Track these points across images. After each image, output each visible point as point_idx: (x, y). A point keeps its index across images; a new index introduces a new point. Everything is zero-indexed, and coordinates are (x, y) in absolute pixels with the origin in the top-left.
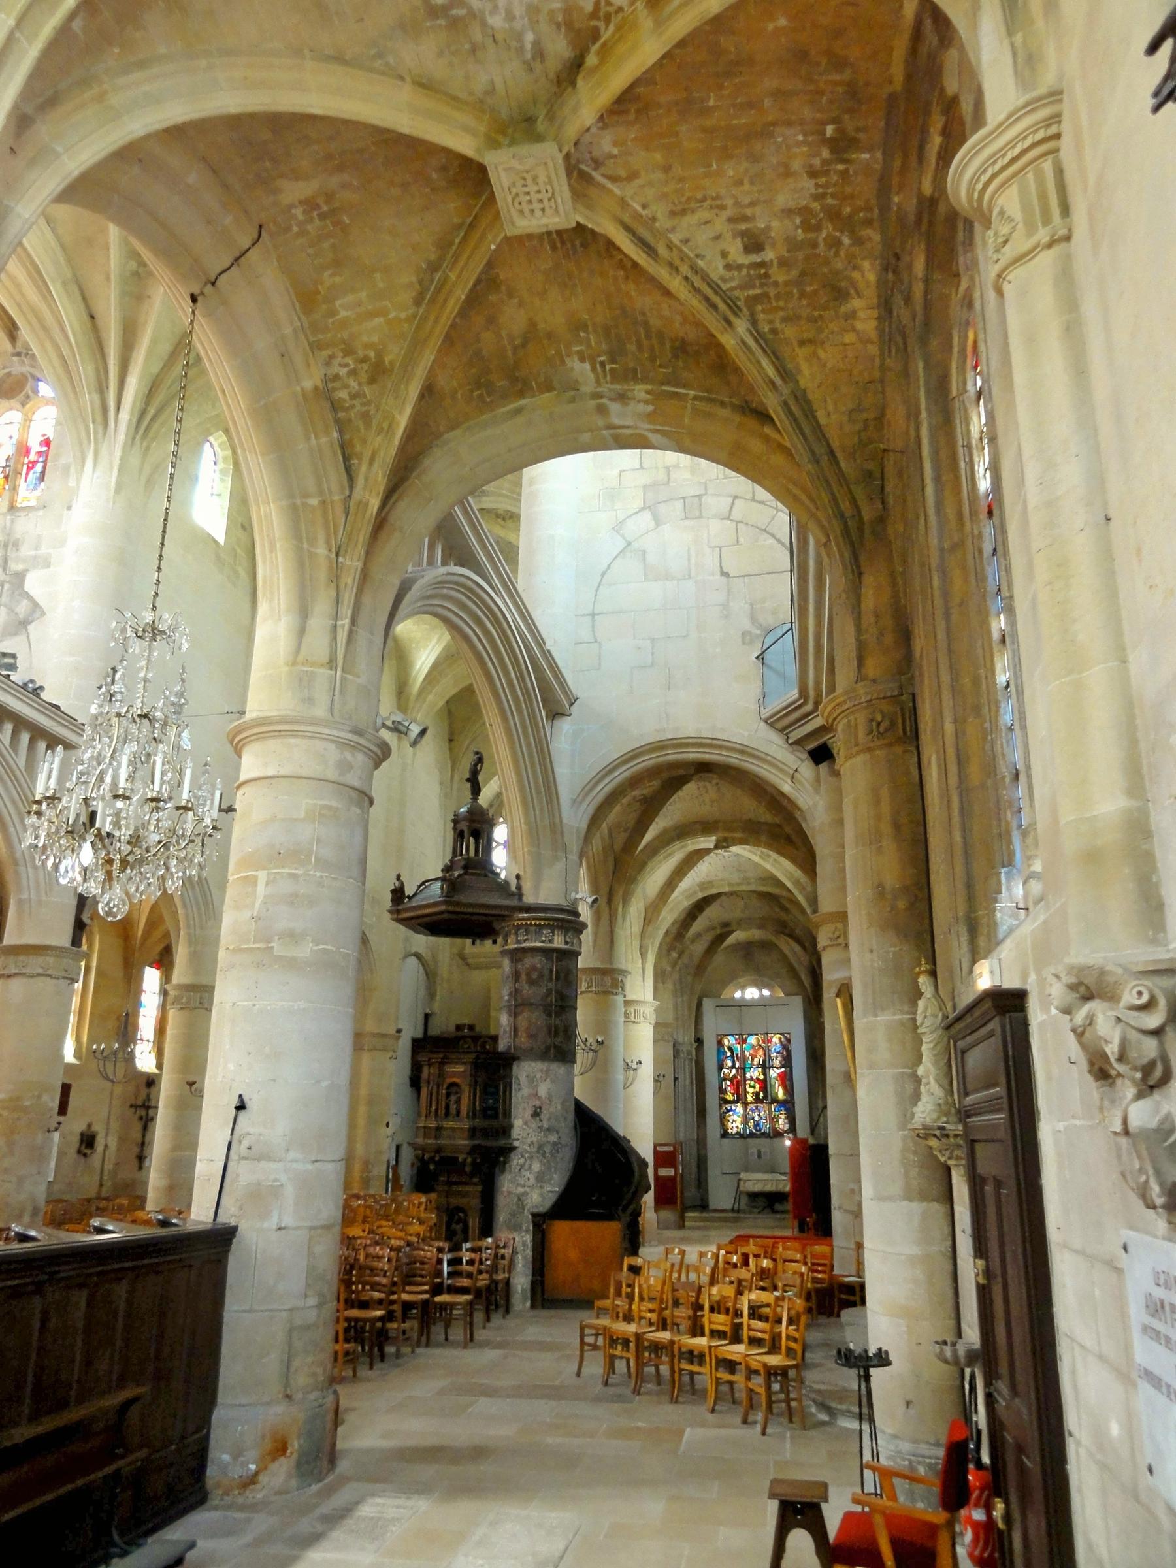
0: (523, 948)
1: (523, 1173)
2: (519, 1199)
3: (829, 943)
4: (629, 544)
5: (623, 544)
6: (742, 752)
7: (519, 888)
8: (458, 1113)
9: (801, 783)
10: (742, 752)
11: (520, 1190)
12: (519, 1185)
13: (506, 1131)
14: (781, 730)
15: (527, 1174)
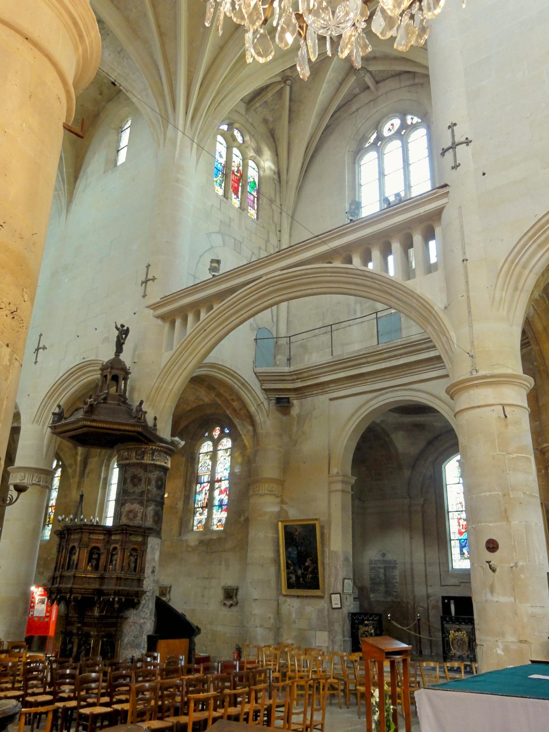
0: (156, 465)
1: (144, 610)
2: (141, 627)
3: (268, 492)
4: (212, 248)
5: (210, 247)
6: (243, 384)
7: (155, 425)
8: (135, 570)
9: (261, 410)
10: (243, 384)
11: (142, 621)
12: (141, 618)
13: (140, 581)
14: (260, 381)
15: (147, 611)
